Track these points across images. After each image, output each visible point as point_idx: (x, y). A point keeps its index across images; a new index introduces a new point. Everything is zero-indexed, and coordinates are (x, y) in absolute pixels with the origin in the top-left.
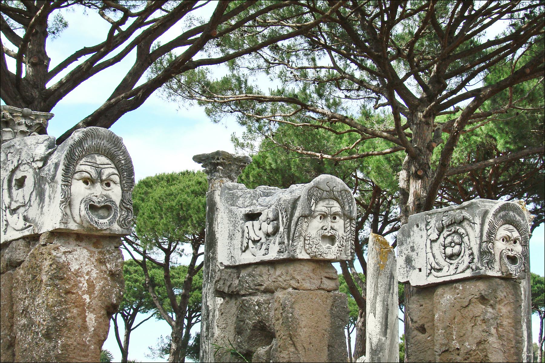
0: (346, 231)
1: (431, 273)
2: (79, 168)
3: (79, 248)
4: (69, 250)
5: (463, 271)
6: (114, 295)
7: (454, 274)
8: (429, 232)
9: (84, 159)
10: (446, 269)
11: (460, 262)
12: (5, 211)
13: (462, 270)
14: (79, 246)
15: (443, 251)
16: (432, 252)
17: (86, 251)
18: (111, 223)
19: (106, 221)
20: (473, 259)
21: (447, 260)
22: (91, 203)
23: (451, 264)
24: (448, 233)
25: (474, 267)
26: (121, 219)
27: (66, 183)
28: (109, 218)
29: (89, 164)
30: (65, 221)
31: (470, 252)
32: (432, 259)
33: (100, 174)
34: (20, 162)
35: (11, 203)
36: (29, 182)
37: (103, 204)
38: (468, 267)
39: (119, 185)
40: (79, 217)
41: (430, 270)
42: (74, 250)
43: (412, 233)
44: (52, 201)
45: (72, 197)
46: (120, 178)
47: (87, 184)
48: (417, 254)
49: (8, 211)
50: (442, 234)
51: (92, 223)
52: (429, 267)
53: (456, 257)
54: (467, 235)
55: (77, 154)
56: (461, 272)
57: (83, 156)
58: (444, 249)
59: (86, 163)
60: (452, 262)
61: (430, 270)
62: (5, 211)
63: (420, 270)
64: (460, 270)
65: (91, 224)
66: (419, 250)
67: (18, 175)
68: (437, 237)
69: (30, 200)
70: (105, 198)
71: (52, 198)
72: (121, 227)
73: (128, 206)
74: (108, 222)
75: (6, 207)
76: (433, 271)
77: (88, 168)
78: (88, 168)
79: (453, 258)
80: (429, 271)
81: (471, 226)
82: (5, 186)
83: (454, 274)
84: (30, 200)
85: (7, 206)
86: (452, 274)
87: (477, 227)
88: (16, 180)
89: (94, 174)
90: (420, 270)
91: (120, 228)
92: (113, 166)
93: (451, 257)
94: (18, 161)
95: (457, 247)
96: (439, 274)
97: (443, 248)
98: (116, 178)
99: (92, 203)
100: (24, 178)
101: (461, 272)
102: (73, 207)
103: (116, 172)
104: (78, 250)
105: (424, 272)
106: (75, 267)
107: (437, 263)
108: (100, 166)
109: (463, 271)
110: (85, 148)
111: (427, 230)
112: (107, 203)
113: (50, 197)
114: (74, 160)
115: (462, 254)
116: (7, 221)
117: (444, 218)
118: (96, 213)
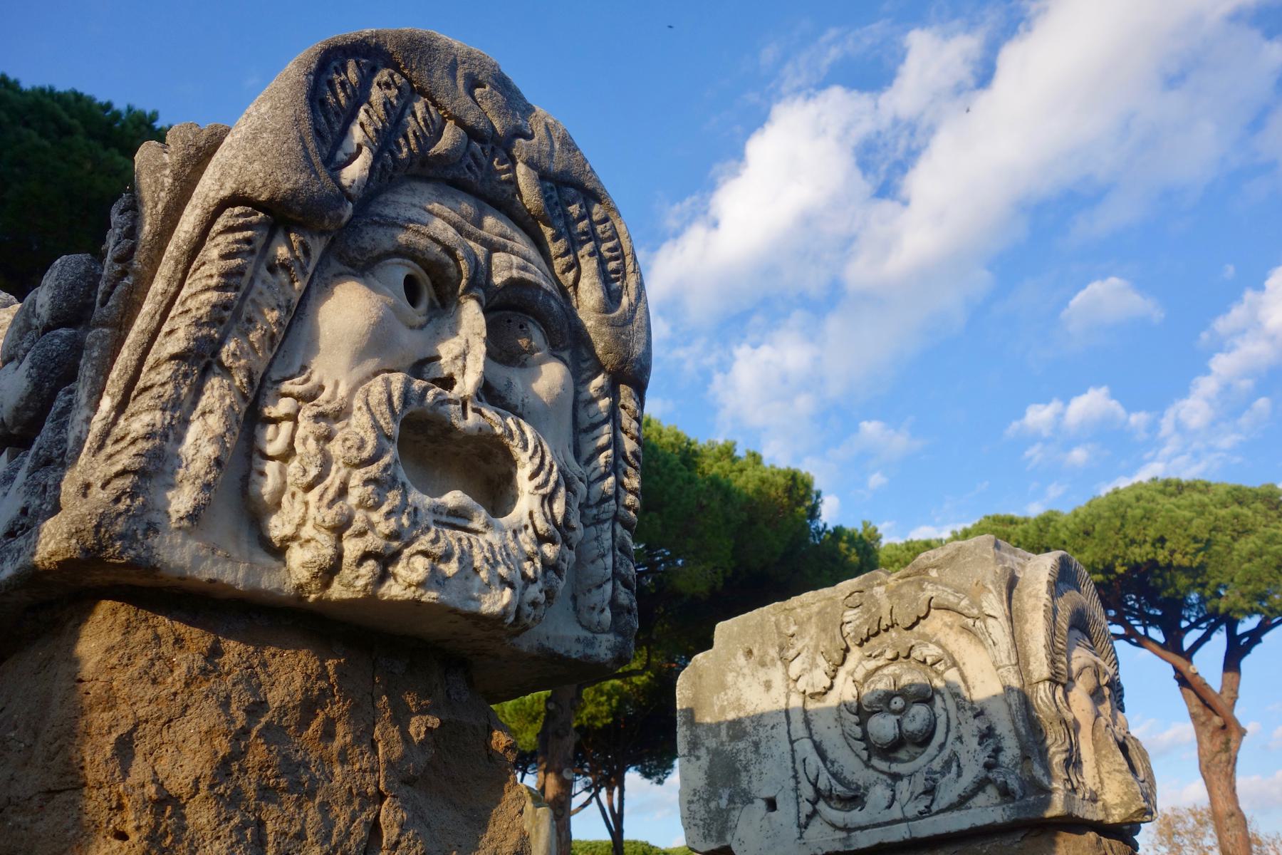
0: (588, 450)
1: (815, 813)
5: (962, 802)
7: (921, 815)
8: (795, 668)
10: (879, 794)
11: (937, 765)
13: (955, 799)
15: (858, 731)
16: (811, 737)
20: (998, 750)
21: (875, 762)
23: (896, 777)
24: (872, 664)
25: (1014, 784)
31: (981, 724)
32: (814, 759)
38: (980, 786)
41: (814, 803)
43: (730, 678)
48: (756, 745)
50: (842, 672)
52: (807, 791)
53: (913, 750)
54: (955, 664)
56: (951, 808)
58: (862, 724)
60: (896, 768)
61: (814, 803)
63: (772, 804)
64: (948, 794)
66: (762, 733)
68: (828, 684)
76: (822, 805)
79: (902, 754)
80: (807, 808)
81: (965, 629)
83: (921, 815)
86: (911, 811)
87: (998, 630)
90: (772, 804)
93: (889, 750)
95: (920, 711)
96: (856, 817)
97: (855, 719)
101: (951, 808)
105: (786, 814)
107: (834, 775)
109: (962, 802)
111: (786, 662)
115: (939, 737)
117: (850, 615)
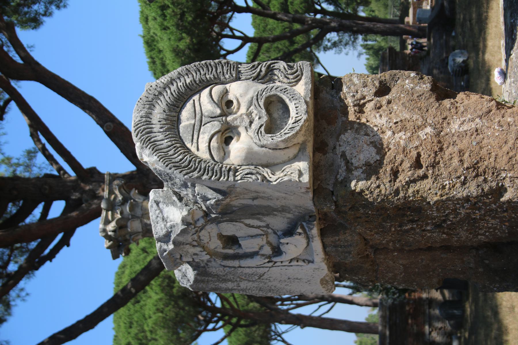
2: (203, 154)
3: (338, 147)
4: (343, 164)
6: (417, 88)
9: (189, 145)
12: (276, 262)
14: (335, 148)
17: (342, 136)
18: (294, 97)
19: (292, 106)
22: (263, 132)
26: (285, 80)
27: (231, 173)
28: (287, 101)
29: (195, 137)
30: (297, 172)
33: (213, 118)
34: (195, 243)
35: (263, 255)
36: (229, 229)
37: (264, 111)
39: (227, 86)
40: (287, 150)
42: (343, 155)
44: (261, 195)
45: (255, 163)
46: (217, 84)
47: (231, 138)
49: (274, 259)
51: (298, 128)
55: (180, 157)
57: (184, 146)
59: (195, 141)
62: (276, 262)
65: (300, 130)
67: (216, 244)
69: (258, 227)
70: (252, 107)
71: (254, 195)
72: (300, 80)
73: (263, 69)
74: (294, 102)
75: (268, 262)
77: (204, 139)
78: (204, 139)
82: (236, 263)
84: (258, 227)
85: (267, 260)
88: (224, 248)
89: (214, 126)
91: (302, 82)
92: (196, 97)
94: (194, 246)
98: (217, 90)
99: (262, 129)
100: (221, 236)
102: (271, 161)
103: (206, 91)
104: (342, 149)
106: (374, 154)
108: (198, 117)
110: (169, 143)
112: (262, 103)
113: (254, 199)
114: (190, 162)
116: (291, 260)
118: (278, 122)
